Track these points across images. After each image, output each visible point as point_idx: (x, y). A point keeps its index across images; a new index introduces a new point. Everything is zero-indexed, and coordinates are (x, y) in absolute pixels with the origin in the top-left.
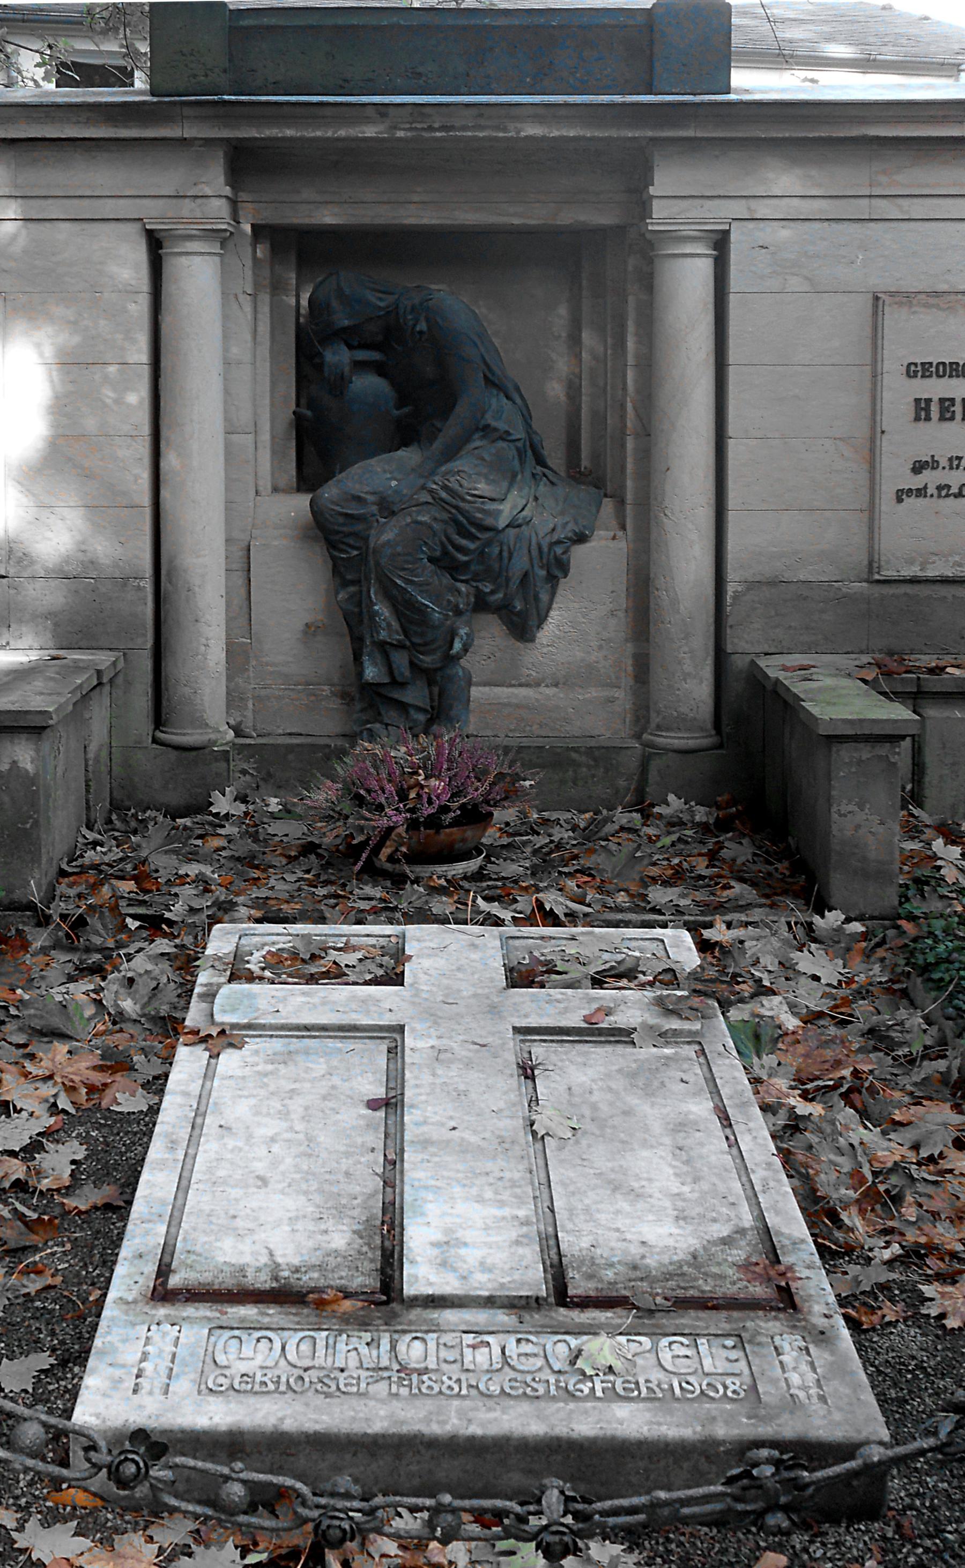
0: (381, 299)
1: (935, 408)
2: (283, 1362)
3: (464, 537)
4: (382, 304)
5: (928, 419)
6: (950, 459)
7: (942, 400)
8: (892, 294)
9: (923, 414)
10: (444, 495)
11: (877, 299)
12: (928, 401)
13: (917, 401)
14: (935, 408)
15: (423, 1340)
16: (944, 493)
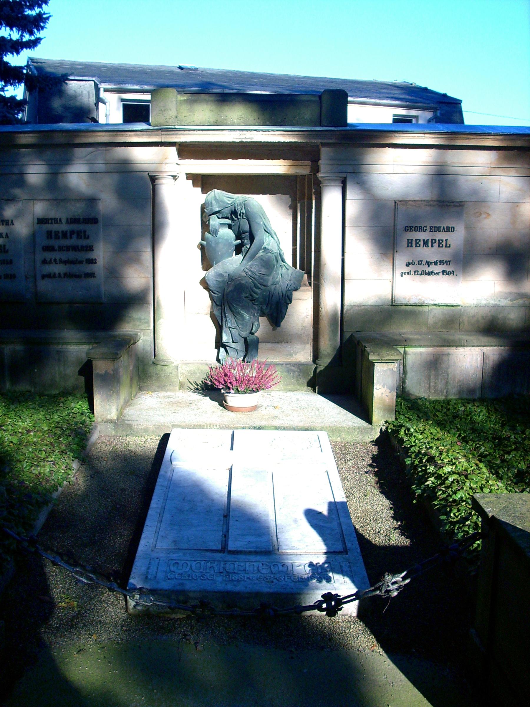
0: (229, 201)
1: (414, 243)
2: (191, 571)
3: (257, 289)
4: (229, 202)
5: (411, 246)
6: (419, 261)
7: (416, 240)
8: (400, 201)
9: (410, 245)
10: (250, 273)
11: (395, 203)
12: (412, 240)
13: (408, 240)
14: (414, 243)
15: (234, 564)
16: (416, 273)
